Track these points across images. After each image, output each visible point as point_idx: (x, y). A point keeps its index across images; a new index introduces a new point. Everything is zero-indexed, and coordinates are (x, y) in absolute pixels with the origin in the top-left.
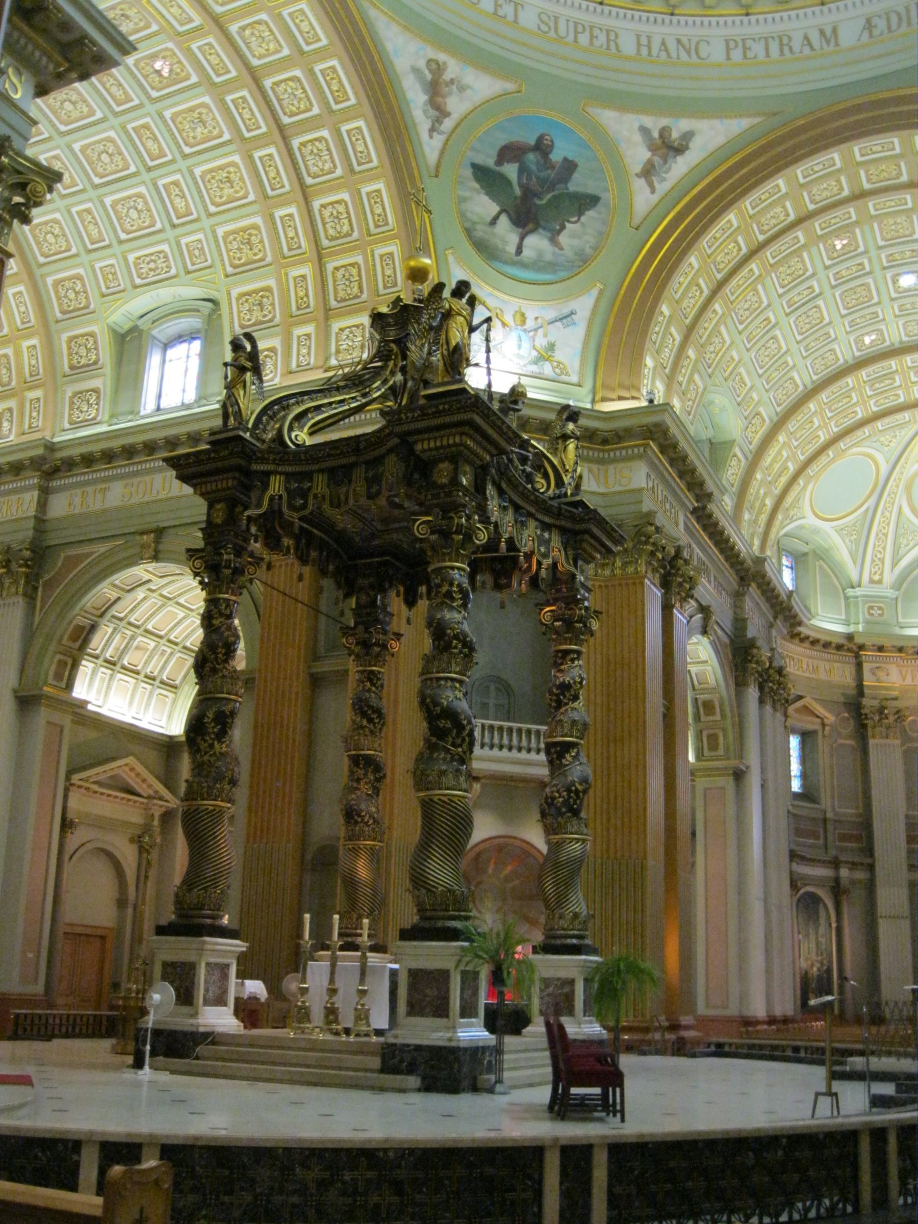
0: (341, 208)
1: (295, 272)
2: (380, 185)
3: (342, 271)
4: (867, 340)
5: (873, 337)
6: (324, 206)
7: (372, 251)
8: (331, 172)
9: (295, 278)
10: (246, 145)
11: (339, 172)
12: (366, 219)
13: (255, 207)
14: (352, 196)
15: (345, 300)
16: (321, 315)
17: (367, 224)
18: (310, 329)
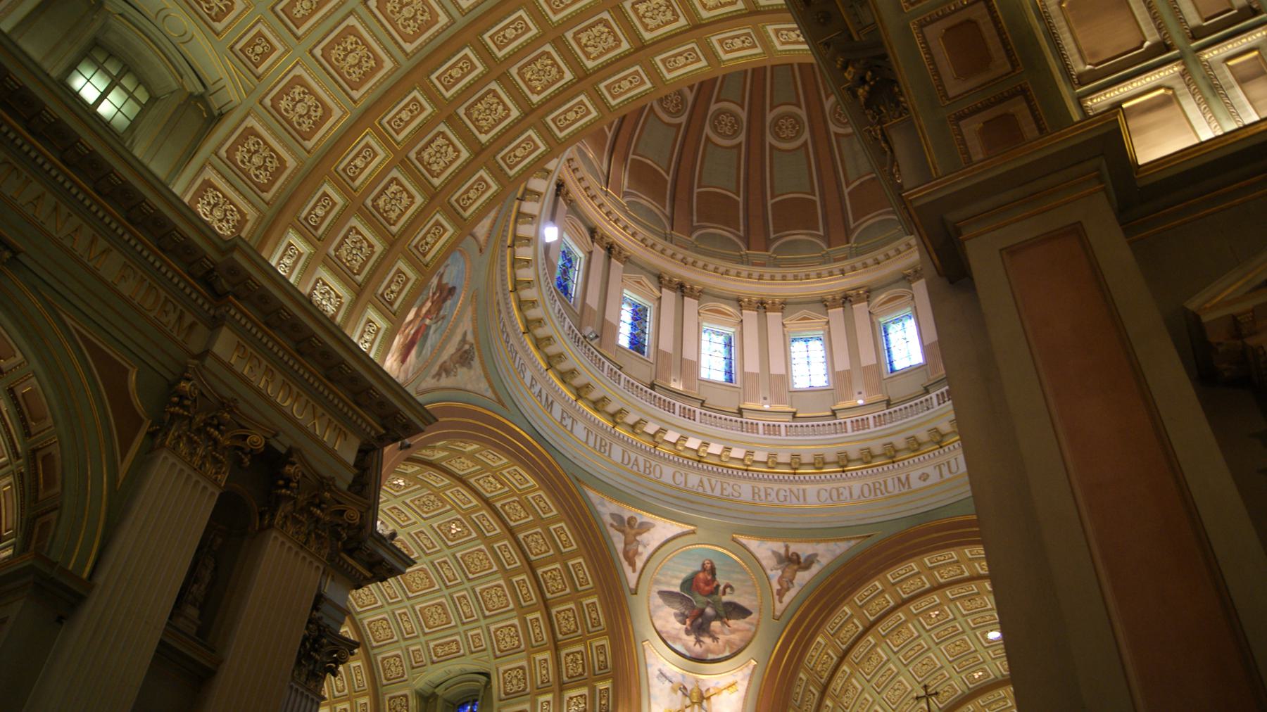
0: (570, 614)
1: (539, 657)
2: (594, 599)
3: (571, 657)
4: (976, 677)
5: (980, 673)
6: (559, 612)
7: (591, 644)
8: (562, 590)
9: (540, 661)
10: (507, 574)
11: (568, 590)
12: (586, 621)
13: (514, 613)
14: (576, 606)
15: (572, 677)
16: (557, 688)
17: (587, 625)
18: (549, 697)
